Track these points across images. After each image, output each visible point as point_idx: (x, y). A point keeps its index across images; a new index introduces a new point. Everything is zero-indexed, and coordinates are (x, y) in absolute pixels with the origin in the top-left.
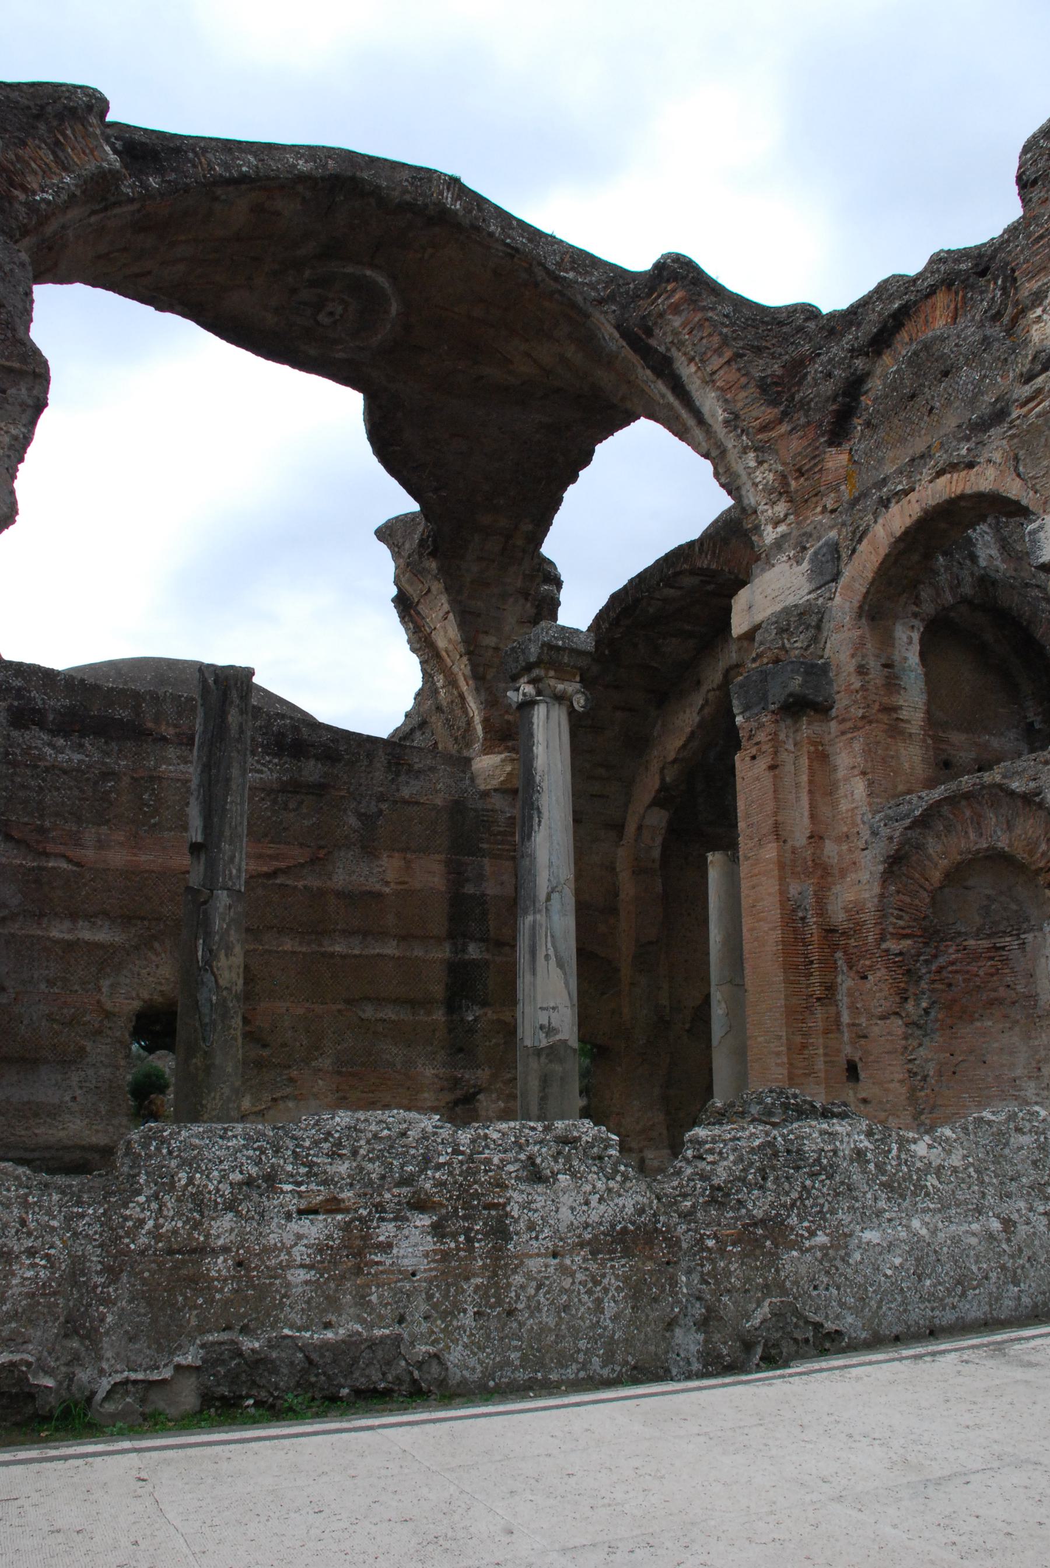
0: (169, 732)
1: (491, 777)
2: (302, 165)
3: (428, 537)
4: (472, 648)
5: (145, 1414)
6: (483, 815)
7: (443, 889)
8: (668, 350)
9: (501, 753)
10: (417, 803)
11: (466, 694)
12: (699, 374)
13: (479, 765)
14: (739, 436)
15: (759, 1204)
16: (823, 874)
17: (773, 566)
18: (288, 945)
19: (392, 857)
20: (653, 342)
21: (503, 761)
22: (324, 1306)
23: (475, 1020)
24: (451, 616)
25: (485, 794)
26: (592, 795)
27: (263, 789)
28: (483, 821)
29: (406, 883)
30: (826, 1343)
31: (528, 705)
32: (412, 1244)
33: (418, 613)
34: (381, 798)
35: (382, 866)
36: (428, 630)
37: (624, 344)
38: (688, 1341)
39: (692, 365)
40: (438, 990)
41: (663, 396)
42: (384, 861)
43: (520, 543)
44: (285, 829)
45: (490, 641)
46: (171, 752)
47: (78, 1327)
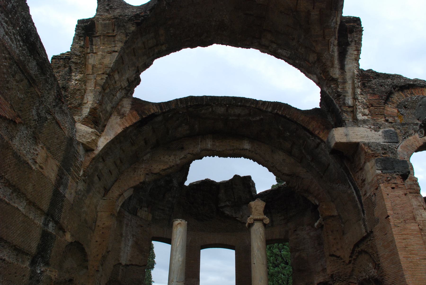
1: (84, 137)
3: (142, 16)
6: (76, 154)
7: (54, 182)
8: (352, 41)
9: (91, 128)
10: (60, 126)
11: (88, 91)
12: (356, 56)
13: (80, 128)
14: (358, 82)
17: (359, 127)
19: (43, 149)
20: (349, 36)
21: (92, 132)
23: (40, 273)
24: (116, 54)
25: (79, 143)
26: (110, 171)
27: (9, 54)
28: (75, 156)
29: (42, 169)
33: (92, 41)
35: (36, 150)
36: (89, 51)
37: (338, 28)
39: (356, 52)
40: (33, 246)
41: (333, 51)
42: (39, 148)
43: (156, 50)
44: (8, 89)
45: (117, 77)
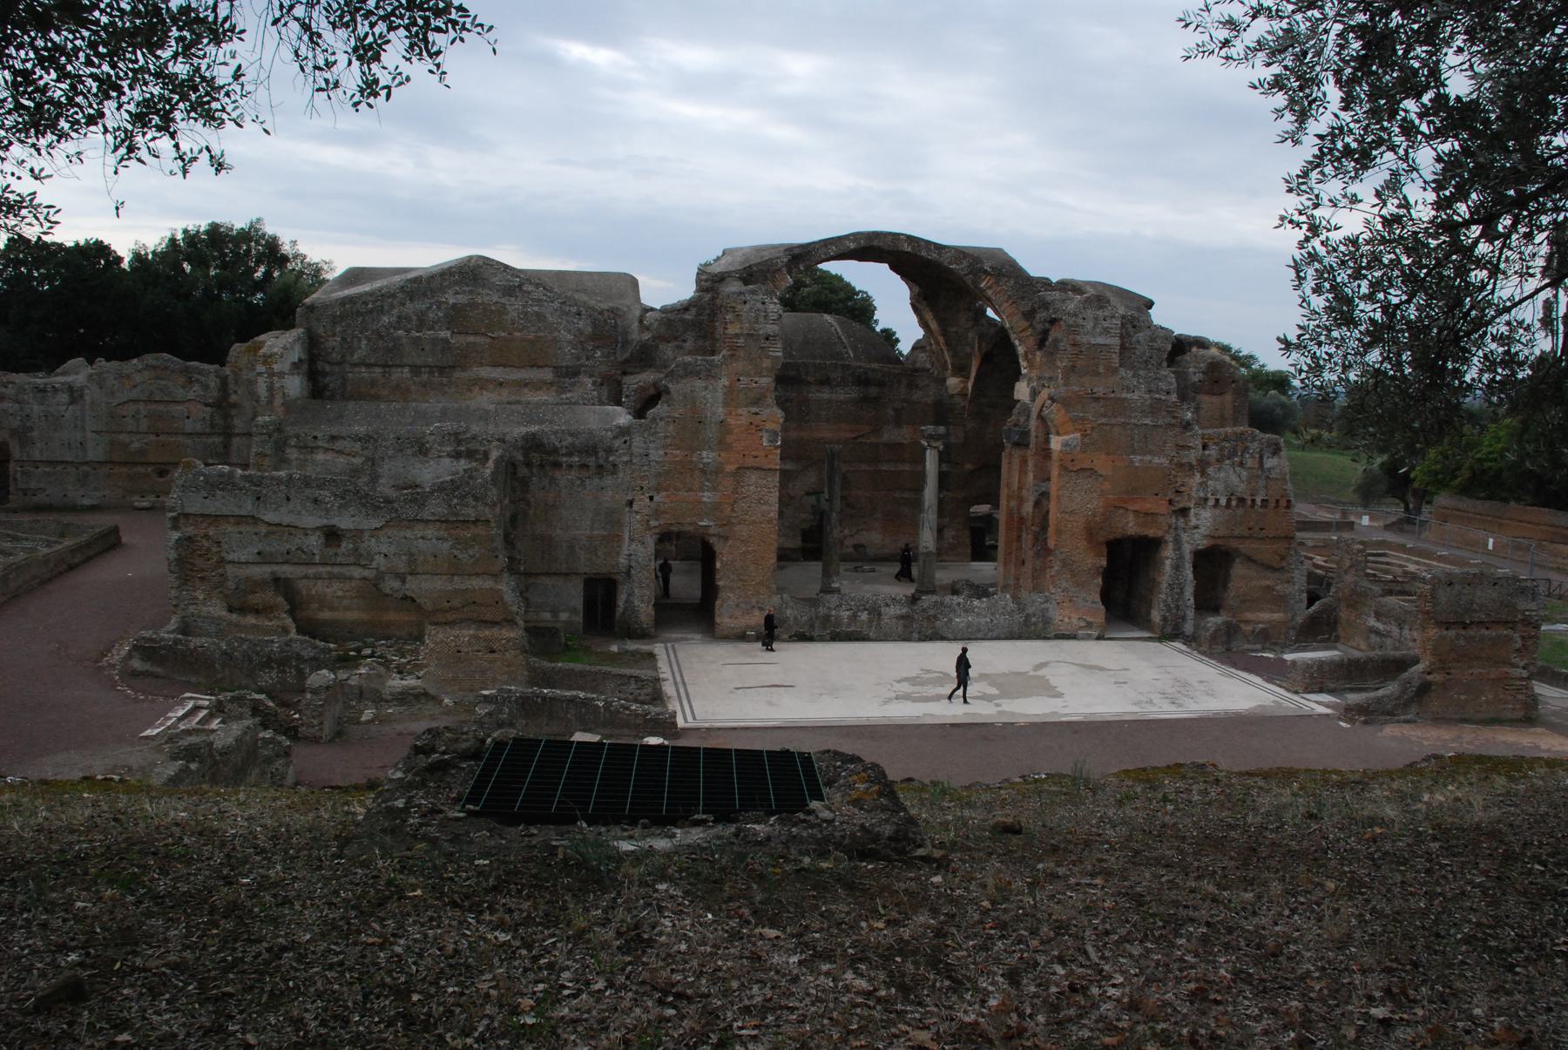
0: (811, 379)
2: (852, 246)
4: (945, 333)
5: (822, 639)
15: (932, 612)
16: (1021, 500)
18: (864, 467)
22: (849, 625)
25: (952, 396)
30: (943, 638)
31: (925, 449)
32: (864, 616)
34: (904, 401)
38: (916, 635)
46: (813, 388)
47: (812, 626)
